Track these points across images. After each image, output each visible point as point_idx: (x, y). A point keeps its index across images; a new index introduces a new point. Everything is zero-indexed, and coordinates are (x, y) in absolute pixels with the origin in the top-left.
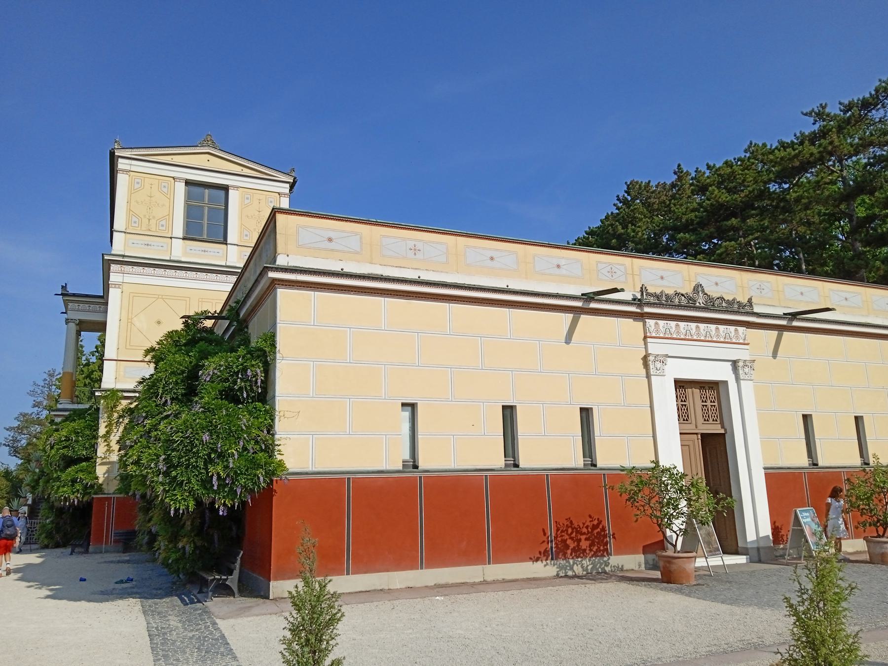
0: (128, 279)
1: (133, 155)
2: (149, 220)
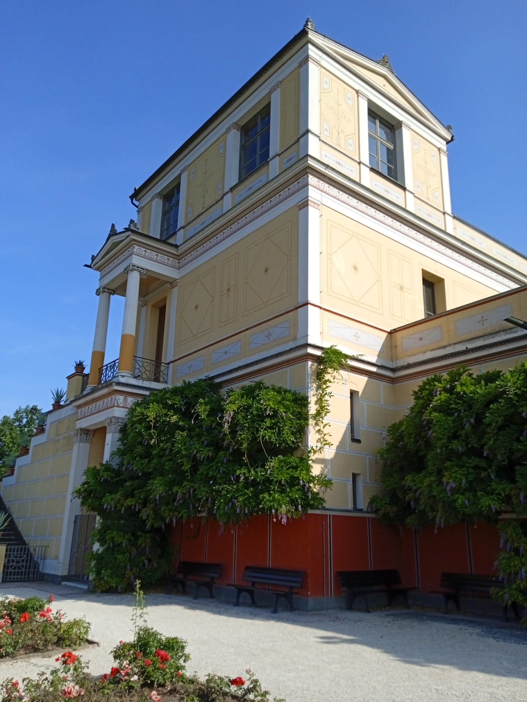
0: (327, 200)
1: (325, 45)
2: (339, 133)
